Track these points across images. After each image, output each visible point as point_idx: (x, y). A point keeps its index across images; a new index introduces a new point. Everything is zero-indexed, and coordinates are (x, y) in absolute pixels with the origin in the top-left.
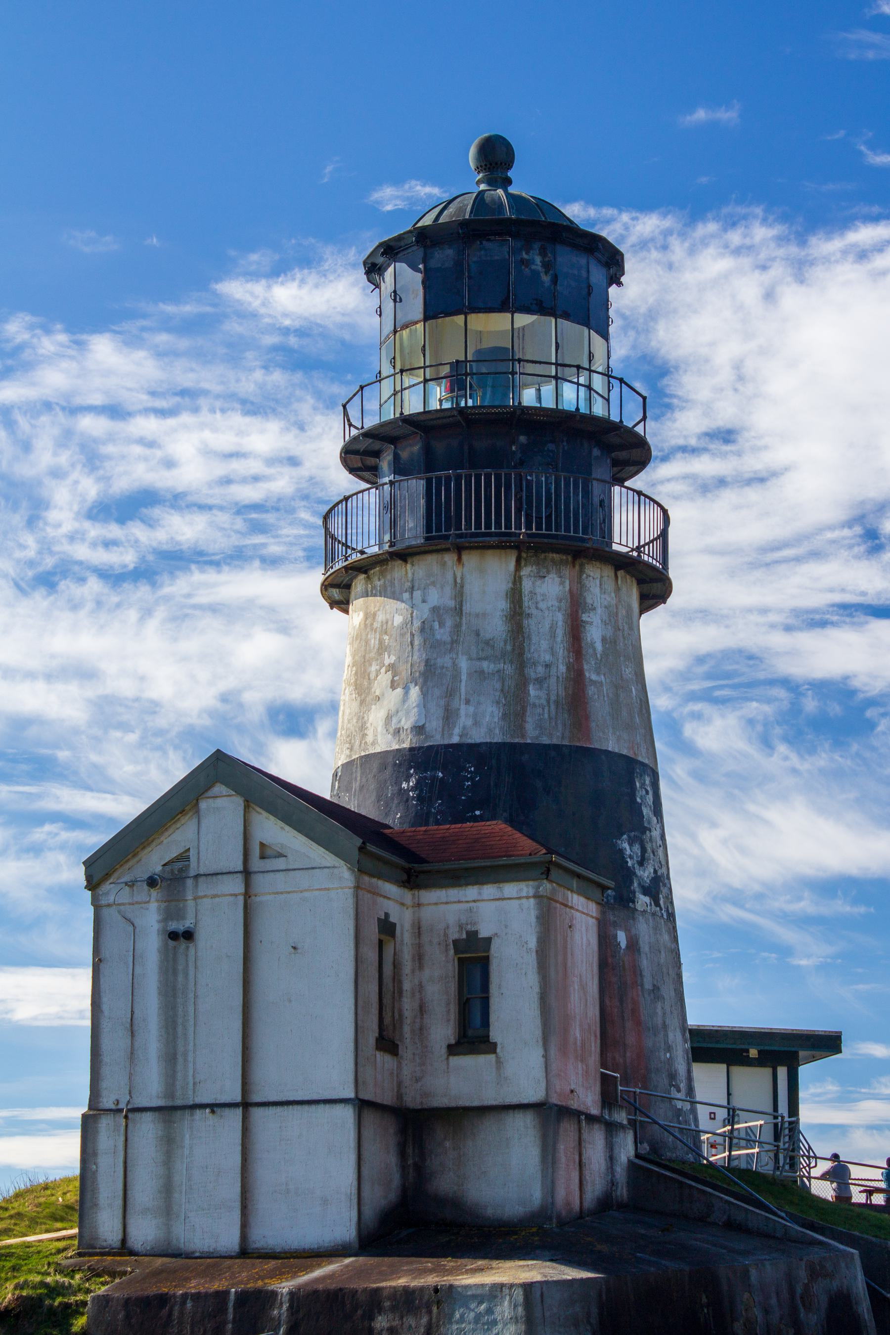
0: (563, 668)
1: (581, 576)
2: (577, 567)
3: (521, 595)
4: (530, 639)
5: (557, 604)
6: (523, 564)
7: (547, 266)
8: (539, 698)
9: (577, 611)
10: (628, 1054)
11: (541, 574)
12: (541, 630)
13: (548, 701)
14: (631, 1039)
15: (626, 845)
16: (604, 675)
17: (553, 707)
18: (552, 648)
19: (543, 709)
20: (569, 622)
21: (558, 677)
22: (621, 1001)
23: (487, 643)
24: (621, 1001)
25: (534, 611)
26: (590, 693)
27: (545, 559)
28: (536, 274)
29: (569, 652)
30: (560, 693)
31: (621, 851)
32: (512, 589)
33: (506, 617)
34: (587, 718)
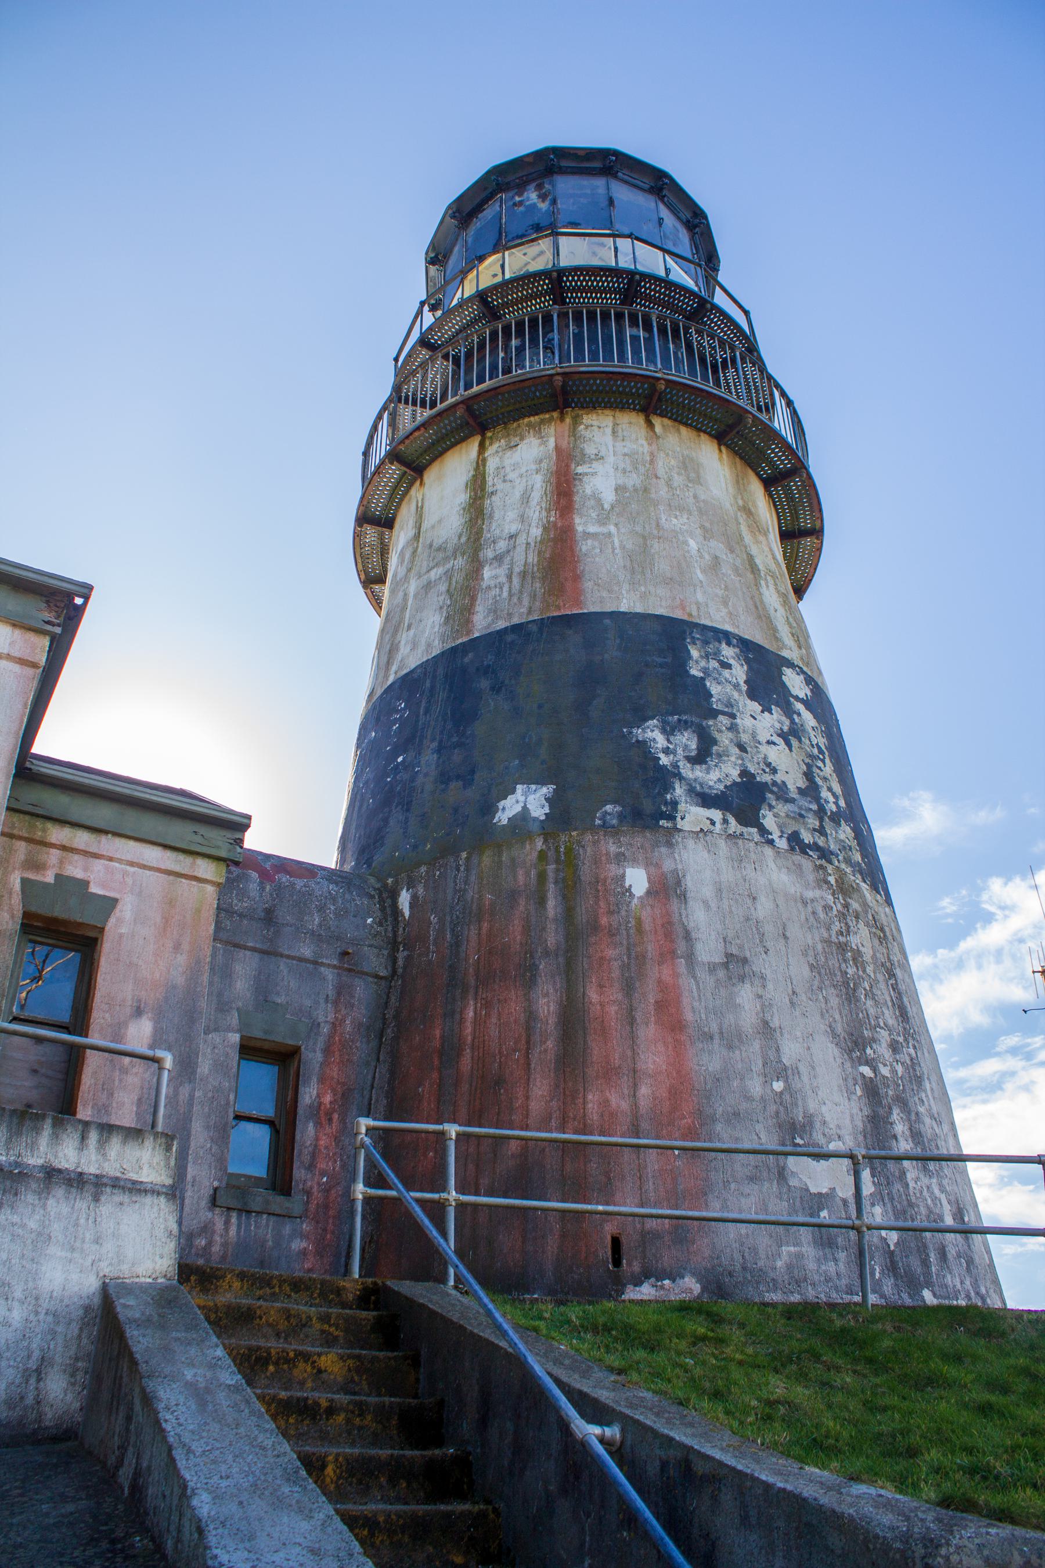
0: (536, 532)
1: (574, 429)
2: (568, 420)
3: (484, 477)
4: (491, 517)
5: (534, 467)
6: (487, 443)
7: (543, 197)
8: (496, 577)
9: (568, 466)
10: (644, 1090)
11: (512, 444)
12: (508, 502)
13: (510, 577)
14: (653, 1058)
15: (660, 740)
16: (616, 525)
17: (516, 581)
18: (522, 516)
19: (501, 588)
20: (553, 480)
21: (528, 544)
22: (628, 988)
23: (439, 549)
24: (628, 988)
25: (500, 486)
26: (584, 548)
27: (519, 426)
28: (534, 205)
29: (548, 511)
30: (530, 560)
31: (643, 746)
32: (474, 476)
33: (464, 509)
34: (577, 578)
